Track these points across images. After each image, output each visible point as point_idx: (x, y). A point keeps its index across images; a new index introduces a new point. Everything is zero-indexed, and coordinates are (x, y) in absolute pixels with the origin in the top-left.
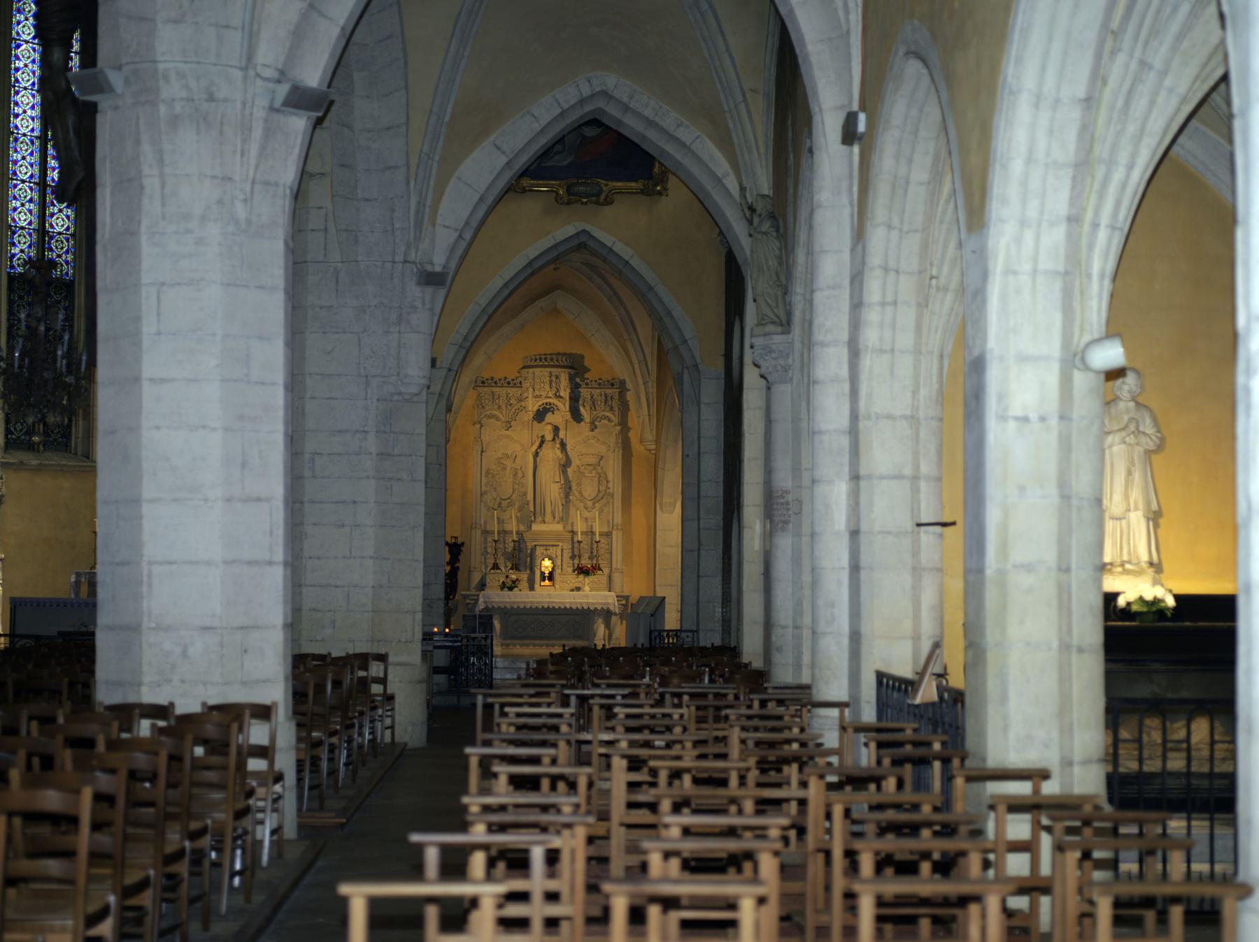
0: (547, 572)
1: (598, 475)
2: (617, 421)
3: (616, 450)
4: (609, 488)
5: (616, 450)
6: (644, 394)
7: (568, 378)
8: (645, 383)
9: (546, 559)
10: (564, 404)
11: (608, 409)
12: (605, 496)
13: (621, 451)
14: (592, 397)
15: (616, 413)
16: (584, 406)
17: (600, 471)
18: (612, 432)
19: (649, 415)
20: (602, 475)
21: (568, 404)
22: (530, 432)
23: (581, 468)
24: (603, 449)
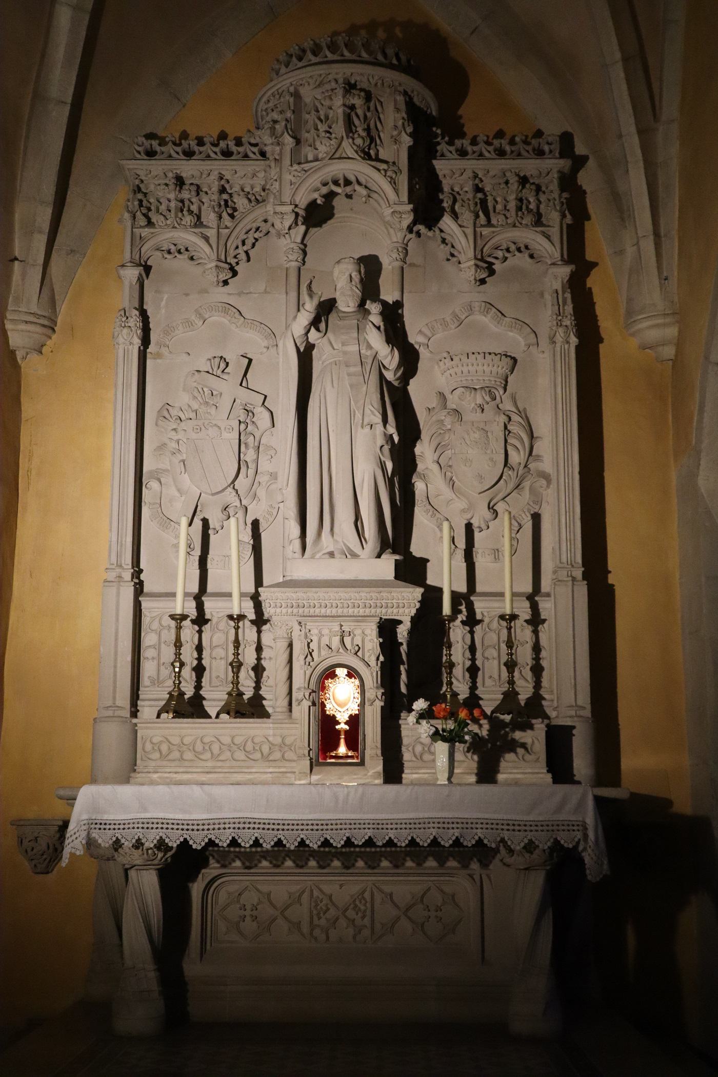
0: (342, 717)
1: (503, 419)
2: (557, 255)
3: (559, 338)
4: (538, 458)
5: (559, 338)
6: (641, 164)
7: (403, 107)
8: (640, 132)
9: (341, 672)
10: (393, 182)
11: (528, 219)
12: (527, 484)
13: (574, 340)
14: (478, 189)
15: (555, 232)
16: (455, 216)
17: (508, 406)
18: (542, 295)
19: (657, 235)
20: (515, 418)
21: (403, 181)
22: (293, 295)
23: (449, 396)
24: (516, 342)
